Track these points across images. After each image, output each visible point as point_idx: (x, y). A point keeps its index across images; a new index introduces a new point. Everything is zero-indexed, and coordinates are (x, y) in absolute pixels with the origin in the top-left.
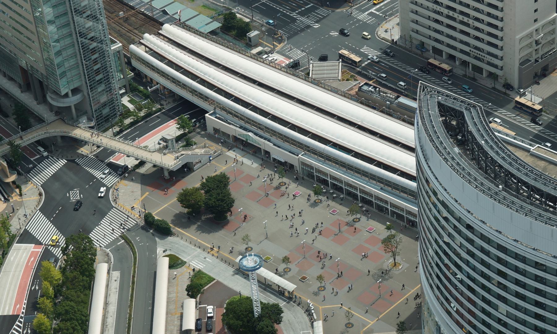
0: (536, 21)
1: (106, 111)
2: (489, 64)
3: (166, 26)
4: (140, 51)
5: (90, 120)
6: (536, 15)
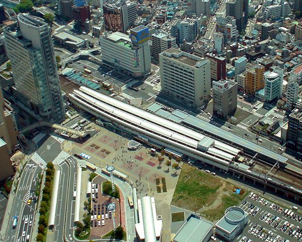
3: (81, 87)
4: (72, 96)
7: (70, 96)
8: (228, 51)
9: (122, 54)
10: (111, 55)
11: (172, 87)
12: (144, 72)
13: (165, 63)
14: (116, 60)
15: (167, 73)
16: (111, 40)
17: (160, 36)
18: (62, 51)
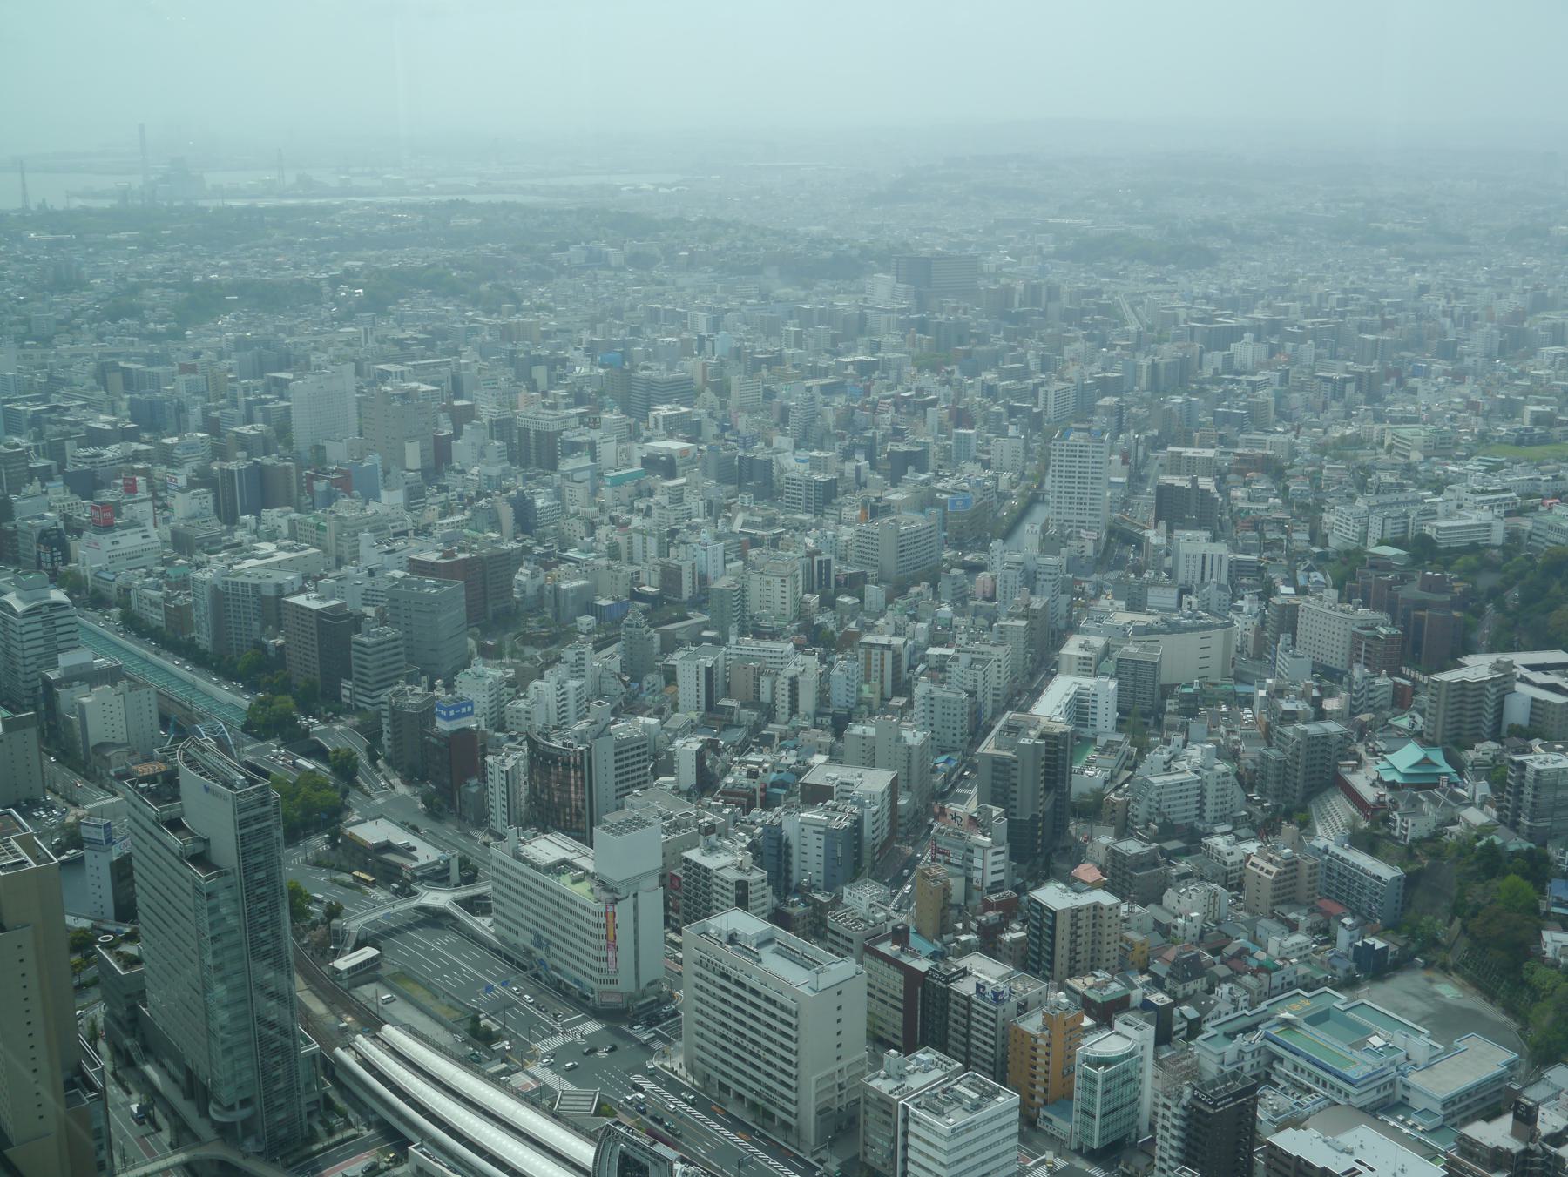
1: (283, 1132)
2: (782, 1109)
3: (387, 1028)
4: (348, 1058)
5: (258, 1141)
6: (839, 1052)
7: (337, 1059)
8: (963, 938)
9: (560, 916)
10: (523, 916)
11: (723, 1061)
12: (633, 989)
13: (700, 964)
14: (538, 936)
15: (707, 1004)
16: (524, 860)
17: (710, 862)
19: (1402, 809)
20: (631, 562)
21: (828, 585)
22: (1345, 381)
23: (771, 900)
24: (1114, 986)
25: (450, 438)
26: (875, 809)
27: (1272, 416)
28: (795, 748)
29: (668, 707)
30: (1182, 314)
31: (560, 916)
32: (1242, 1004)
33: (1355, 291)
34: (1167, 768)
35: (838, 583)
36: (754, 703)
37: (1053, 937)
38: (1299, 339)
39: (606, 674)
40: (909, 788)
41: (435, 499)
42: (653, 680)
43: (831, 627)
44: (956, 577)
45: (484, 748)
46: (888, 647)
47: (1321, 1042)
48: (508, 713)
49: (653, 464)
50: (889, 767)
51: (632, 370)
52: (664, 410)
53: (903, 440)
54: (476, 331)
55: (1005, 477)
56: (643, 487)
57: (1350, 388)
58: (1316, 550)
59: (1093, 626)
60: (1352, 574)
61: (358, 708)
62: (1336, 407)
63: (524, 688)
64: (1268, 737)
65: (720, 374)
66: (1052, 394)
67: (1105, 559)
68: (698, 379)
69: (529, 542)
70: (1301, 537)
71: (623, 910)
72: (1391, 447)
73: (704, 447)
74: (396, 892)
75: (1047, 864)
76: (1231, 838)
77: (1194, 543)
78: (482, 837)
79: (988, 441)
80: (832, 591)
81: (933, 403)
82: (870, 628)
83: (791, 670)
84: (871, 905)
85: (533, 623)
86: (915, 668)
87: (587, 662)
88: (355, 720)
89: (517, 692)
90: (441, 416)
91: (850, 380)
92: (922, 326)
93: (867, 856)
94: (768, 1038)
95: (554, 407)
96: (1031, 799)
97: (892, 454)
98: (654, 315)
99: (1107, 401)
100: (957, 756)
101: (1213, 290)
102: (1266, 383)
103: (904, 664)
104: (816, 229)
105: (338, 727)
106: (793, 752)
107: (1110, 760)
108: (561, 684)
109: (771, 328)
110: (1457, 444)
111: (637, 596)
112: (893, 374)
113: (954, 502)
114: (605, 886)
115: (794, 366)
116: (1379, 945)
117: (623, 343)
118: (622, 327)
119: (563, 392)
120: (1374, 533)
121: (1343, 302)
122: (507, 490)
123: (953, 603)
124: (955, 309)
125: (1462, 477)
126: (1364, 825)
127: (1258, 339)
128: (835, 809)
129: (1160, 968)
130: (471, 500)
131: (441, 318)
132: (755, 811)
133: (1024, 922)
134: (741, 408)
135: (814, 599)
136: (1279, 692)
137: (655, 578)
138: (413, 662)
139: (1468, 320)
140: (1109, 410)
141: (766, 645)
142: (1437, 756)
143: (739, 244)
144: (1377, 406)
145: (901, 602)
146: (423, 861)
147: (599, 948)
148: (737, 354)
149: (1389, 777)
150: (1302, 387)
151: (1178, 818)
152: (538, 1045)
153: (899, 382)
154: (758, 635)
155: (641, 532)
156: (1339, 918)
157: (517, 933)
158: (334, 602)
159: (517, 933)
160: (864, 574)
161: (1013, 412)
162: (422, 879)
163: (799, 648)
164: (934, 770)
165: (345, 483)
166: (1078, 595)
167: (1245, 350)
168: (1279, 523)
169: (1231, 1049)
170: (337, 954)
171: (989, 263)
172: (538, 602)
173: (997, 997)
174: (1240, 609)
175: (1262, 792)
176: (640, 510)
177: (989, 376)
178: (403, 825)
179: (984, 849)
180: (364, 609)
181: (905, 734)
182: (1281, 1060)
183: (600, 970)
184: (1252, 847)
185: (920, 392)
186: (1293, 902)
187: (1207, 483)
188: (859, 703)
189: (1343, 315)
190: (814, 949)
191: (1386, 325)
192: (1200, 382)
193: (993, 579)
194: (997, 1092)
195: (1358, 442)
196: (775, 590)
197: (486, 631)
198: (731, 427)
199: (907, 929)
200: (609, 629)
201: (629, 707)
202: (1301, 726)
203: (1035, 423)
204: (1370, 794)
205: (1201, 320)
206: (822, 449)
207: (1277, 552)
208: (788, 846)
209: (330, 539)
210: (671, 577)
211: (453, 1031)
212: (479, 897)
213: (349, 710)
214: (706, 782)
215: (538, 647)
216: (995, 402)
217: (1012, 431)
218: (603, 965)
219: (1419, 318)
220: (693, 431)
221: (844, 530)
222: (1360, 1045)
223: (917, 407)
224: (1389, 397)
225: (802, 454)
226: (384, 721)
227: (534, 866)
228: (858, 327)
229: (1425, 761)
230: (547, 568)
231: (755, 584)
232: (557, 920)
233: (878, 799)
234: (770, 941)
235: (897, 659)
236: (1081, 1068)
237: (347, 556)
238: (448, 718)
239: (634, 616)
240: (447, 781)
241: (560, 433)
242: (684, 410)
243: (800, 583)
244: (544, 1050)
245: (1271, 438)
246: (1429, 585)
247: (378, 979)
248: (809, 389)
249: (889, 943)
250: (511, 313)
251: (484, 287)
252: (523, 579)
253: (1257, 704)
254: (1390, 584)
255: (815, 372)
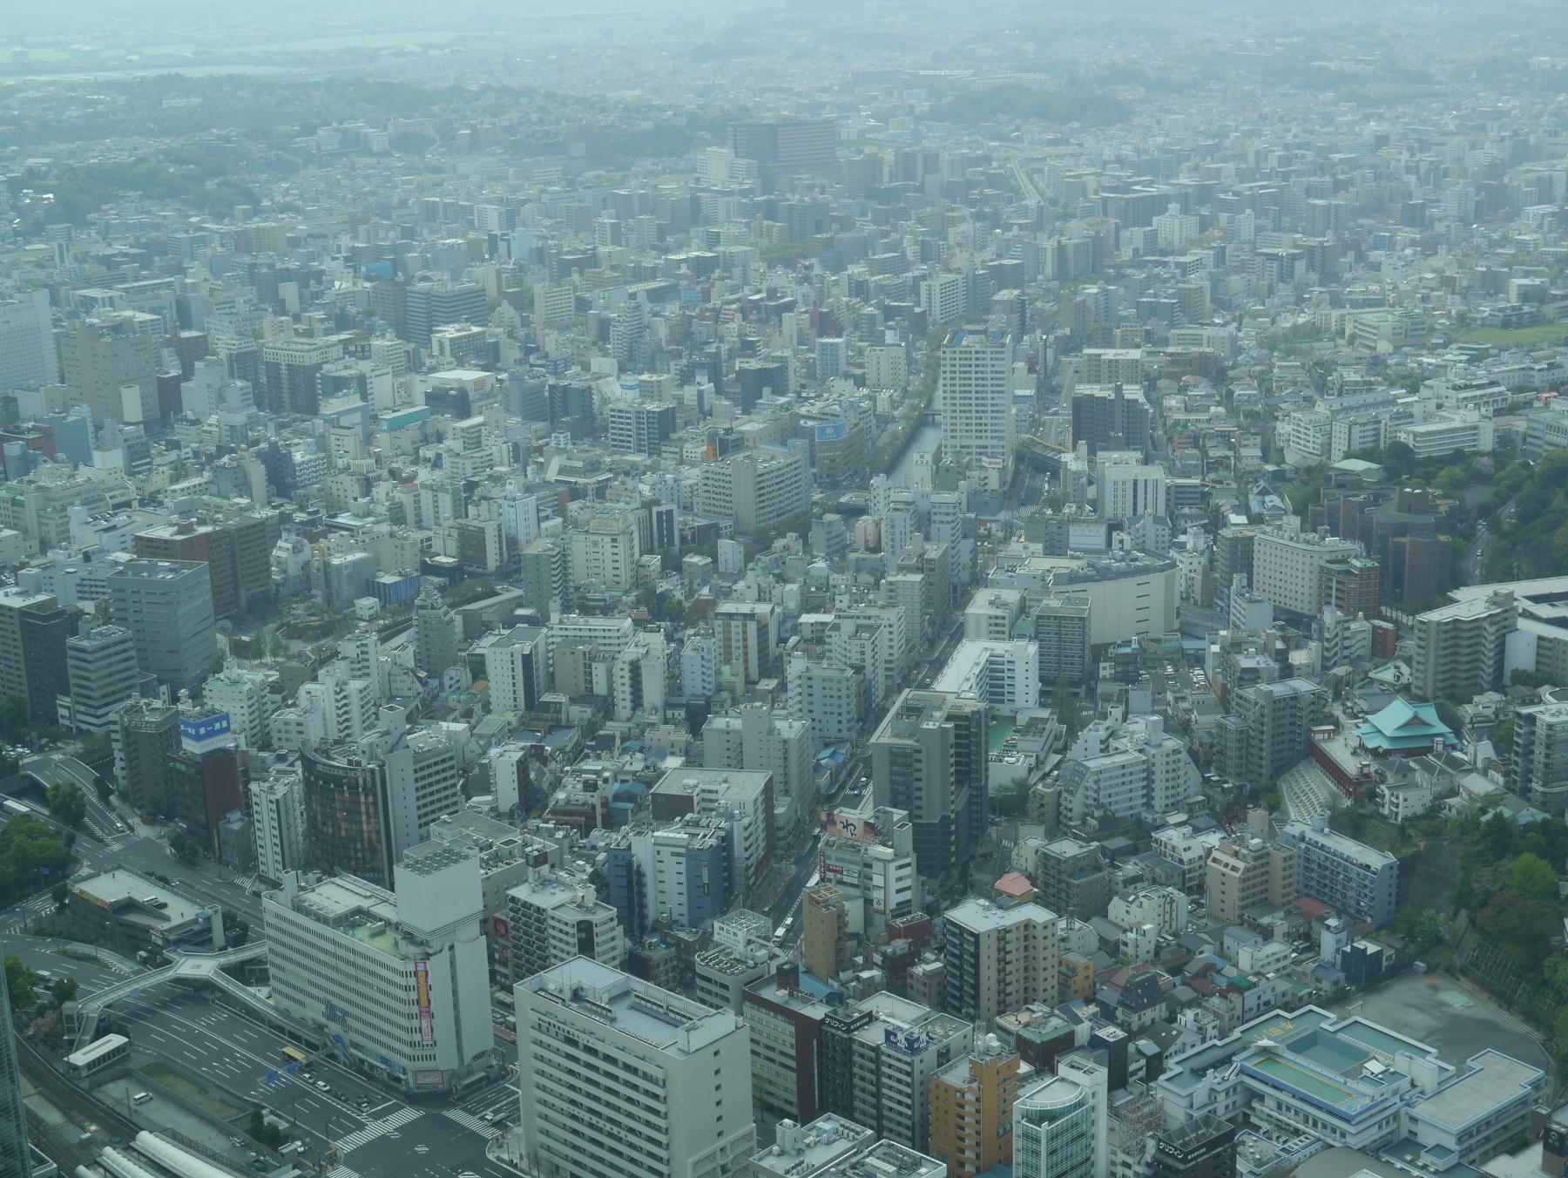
0: (720, 1134)
8: (865, 975)
9: (357, 979)
10: (311, 983)
11: (575, 1147)
12: (455, 1066)
14: (331, 1007)
15: (551, 1077)
16: (307, 912)
17: (545, 900)
18: (94, 960)
19: (1391, 779)
20: (419, 525)
21: (671, 543)
22: (1294, 257)
23: (622, 943)
24: (1055, 1022)
25: (177, 380)
26: (746, 821)
27: (1208, 305)
28: (641, 750)
29: (478, 708)
30: (1091, 183)
31: (357, 979)
32: (1211, 1032)
33: (1300, 146)
34: (1105, 749)
35: (683, 539)
36: (586, 696)
37: (976, 966)
38: (1234, 208)
39: (397, 671)
40: (787, 793)
41: (163, 460)
42: (458, 674)
43: (679, 595)
44: (830, 523)
45: (246, 773)
46: (751, 616)
47: (1309, 1073)
48: (274, 727)
49: (437, 399)
50: (760, 767)
51: (409, 280)
52: (450, 332)
53: (754, 355)
54: (203, 242)
55: (884, 395)
56: (430, 430)
57: (1300, 266)
58: (1270, 468)
59: (1003, 576)
60: (1315, 496)
61: (80, 731)
62: (1284, 291)
63: (293, 694)
64: (1225, 704)
65: (520, 283)
66: (936, 293)
67: (1014, 492)
68: (492, 291)
69: (288, 508)
70: (1251, 453)
71: (437, 968)
72: (1353, 337)
73: (504, 376)
74: (144, 962)
75: (964, 874)
76: (1187, 829)
77: (1122, 467)
78: (248, 884)
79: (860, 352)
80: (676, 549)
81: (790, 307)
82: (727, 594)
83: (630, 653)
84: (749, 942)
85: (299, 610)
86: (785, 640)
87: (371, 656)
88: (78, 746)
89: (284, 699)
90: (165, 351)
91: (684, 283)
92: (771, 211)
93: (740, 880)
94: (630, 1115)
95: (309, 333)
96: (940, 797)
97: (742, 373)
98: (431, 212)
99: (1005, 294)
100: (844, 750)
101: (1127, 151)
102: (1199, 264)
103: (773, 637)
104: (631, 95)
105: (57, 757)
106: (639, 756)
107: (1034, 744)
108: (341, 686)
109: (580, 222)
110: (1432, 330)
111: (428, 569)
112: (737, 272)
113: (823, 430)
114: (409, 937)
115: (613, 268)
116: (1372, 949)
117: (394, 248)
118: (392, 228)
119: (320, 315)
120: (1339, 445)
121: (1286, 161)
122: (256, 442)
123: (828, 557)
124: (810, 188)
125: (1440, 370)
126: (1347, 803)
127: (1185, 210)
128: (697, 824)
129: (1109, 994)
130: (211, 458)
131: (157, 227)
132: (595, 833)
133: (940, 949)
134: (549, 324)
135: (655, 561)
136: (1236, 646)
137: (452, 546)
138: (148, 669)
139: (1437, 176)
140: (1008, 306)
141: (598, 622)
142: (1429, 714)
143: (535, 117)
144: (1333, 287)
145: (765, 559)
146: (176, 920)
147: (410, 1017)
148: (540, 255)
149: (1371, 745)
150: (1242, 268)
151: (1121, 809)
152: (339, 1144)
153: (746, 282)
154: (587, 610)
155: (431, 487)
156: (1322, 919)
157: (303, 1004)
158: (41, 598)
159: (303, 1004)
160: (715, 526)
161: (889, 313)
162: (178, 943)
163: (638, 623)
164: (817, 768)
165: (46, 443)
166: (982, 538)
167: (1171, 225)
168: (1225, 436)
169: (1201, 1088)
170: (72, 1046)
171: (851, 127)
172: (303, 585)
173: (912, 1046)
174: (1182, 546)
175: (1221, 771)
176: (427, 460)
177: (857, 270)
178: (149, 875)
179: (884, 861)
180: (81, 604)
181: (779, 724)
182: (1261, 1097)
183: (412, 1044)
184: (1213, 839)
185: (772, 293)
186: (1267, 906)
187: (1133, 392)
188: (719, 689)
189: (1286, 176)
190: (679, 1001)
191: (1338, 186)
192: (1119, 267)
193: (877, 524)
194: (918, 1163)
195: (1314, 332)
196: (606, 551)
197: (240, 624)
198: (537, 349)
199: (795, 970)
200: (398, 611)
201: (429, 710)
202: (1264, 687)
203: (918, 325)
204: (1351, 765)
205: (1114, 190)
206: (653, 370)
207: (1222, 473)
208: (641, 874)
209: (30, 515)
210: (471, 542)
211: (229, 1134)
212: (251, 961)
213: (68, 734)
214: (531, 800)
215: (307, 640)
216: (866, 301)
217: (890, 337)
218: (417, 1037)
219: (1378, 177)
220: (488, 356)
221: (688, 470)
222: (1355, 1073)
223: (769, 313)
224: (1347, 276)
225: (630, 379)
226: (116, 745)
227: (319, 918)
228: (693, 213)
229: (1416, 721)
230: (313, 539)
231: (579, 545)
232: (353, 984)
233: (750, 809)
234: (626, 994)
235: (763, 631)
236: (1019, 1126)
237: (53, 537)
238: (198, 738)
239: (428, 595)
240: (201, 817)
241: (319, 367)
242: (475, 329)
243: (636, 542)
244: (347, 1149)
245: (1208, 332)
246: (1409, 505)
247: (127, 1075)
248: (633, 296)
249: (775, 987)
250: (247, 217)
251: (210, 185)
252: (283, 555)
253: (1209, 663)
254: (1361, 507)
255: (639, 274)
